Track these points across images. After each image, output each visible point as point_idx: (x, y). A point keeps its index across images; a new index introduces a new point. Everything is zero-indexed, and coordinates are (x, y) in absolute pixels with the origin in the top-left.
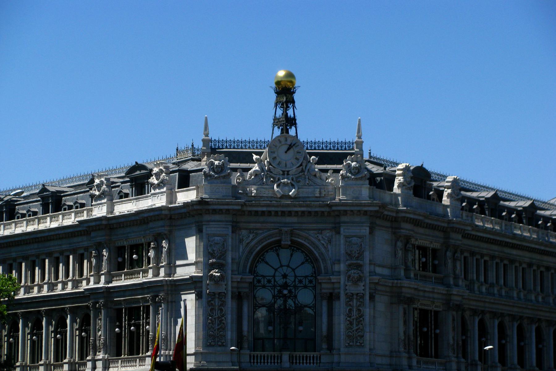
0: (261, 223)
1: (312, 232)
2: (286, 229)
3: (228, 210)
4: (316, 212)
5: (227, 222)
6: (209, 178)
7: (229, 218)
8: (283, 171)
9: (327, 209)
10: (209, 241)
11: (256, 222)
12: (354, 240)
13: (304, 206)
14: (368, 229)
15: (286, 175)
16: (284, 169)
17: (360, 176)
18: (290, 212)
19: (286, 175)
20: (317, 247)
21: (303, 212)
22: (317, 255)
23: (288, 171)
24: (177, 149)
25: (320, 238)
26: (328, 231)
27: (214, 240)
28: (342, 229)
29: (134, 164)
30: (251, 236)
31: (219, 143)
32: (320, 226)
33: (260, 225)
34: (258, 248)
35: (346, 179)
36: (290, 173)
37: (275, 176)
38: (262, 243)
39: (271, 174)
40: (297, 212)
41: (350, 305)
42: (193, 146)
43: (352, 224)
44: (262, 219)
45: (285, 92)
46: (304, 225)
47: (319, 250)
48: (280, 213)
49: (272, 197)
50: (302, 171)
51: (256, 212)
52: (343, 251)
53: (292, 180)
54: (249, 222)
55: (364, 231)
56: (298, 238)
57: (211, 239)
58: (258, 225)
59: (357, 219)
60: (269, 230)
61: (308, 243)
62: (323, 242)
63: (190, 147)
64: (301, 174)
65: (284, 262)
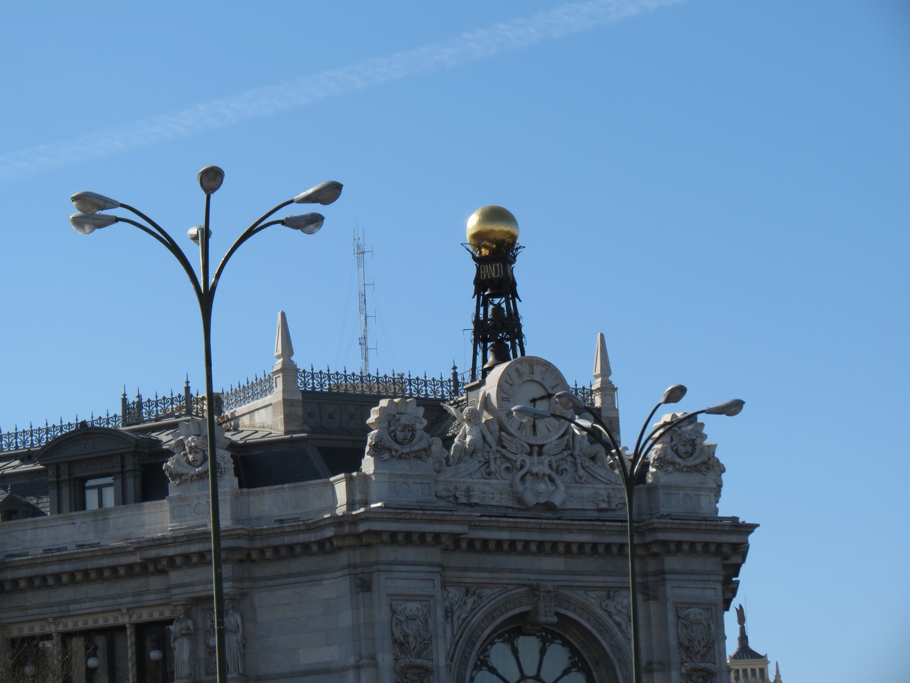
0: (492, 570)
1: (593, 594)
2: (550, 586)
3: (437, 536)
4: (608, 546)
5: (431, 565)
6: (386, 456)
7: (434, 555)
8: (531, 446)
10: (394, 612)
11: (479, 569)
12: (695, 613)
13: (588, 531)
14: (719, 587)
15: (535, 456)
16: (532, 442)
17: (698, 461)
18: (555, 544)
19: (535, 456)
21: (581, 545)
22: (608, 650)
23: (541, 447)
24: (124, 400)
25: (612, 609)
27: (405, 609)
28: (668, 587)
30: (470, 601)
31: (313, 378)
32: (611, 581)
33: (487, 575)
35: (671, 468)
36: (545, 449)
37: (513, 457)
38: (494, 619)
39: (504, 451)
40: (568, 545)
42: (187, 389)
43: (687, 577)
44: (492, 560)
45: (496, 262)
46: (579, 578)
48: (533, 548)
49: (507, 507)
50: (567, 447)
51: (485, 542)
52: (673, 642)
53: (550, 466)
54: (465, 569)
55: (712, 592)
56: (567, 609)
57: (400, 608)
59: (697, 563)
61: (589, 621)
62: (618, 619)
63: (183, 394)
64: (565, 453)
65: (530, 671)
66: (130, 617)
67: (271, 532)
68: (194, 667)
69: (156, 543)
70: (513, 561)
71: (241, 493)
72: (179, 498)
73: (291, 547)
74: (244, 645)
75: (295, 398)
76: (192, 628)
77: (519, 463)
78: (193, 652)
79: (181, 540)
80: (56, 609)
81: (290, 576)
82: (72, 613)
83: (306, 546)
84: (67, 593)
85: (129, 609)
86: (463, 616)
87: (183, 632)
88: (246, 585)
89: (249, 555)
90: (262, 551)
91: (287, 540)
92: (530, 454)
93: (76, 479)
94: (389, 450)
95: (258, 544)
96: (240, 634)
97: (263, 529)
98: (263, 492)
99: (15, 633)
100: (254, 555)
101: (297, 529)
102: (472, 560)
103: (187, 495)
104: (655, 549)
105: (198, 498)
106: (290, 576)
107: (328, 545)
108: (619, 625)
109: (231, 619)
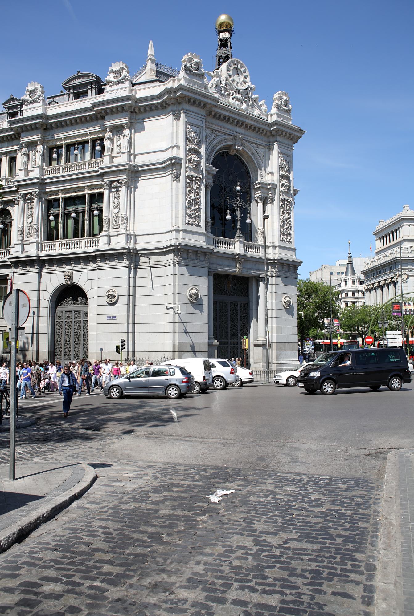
1: (252, 145)
9: (268, 128)
16: (237, 87)
20: (256, 158)
23: (239, 90)
26: (263, 147)
30: (213, 135)
32: (259, 142)
33: (219, 128)
34: (218, 148)
41: (283, 208)
44: (221, 123)
47: (258, 161)
54: (212, 124)
58: (218, 128)
59: (286, 141)
60: (225, 134)
62: (260, 155)
70: (228, 126)
77: (231, 94)
86: (211, 139)
92: (235, 92)
94: (190, 70)
100: (137, 111)
102: (215, 121)
104: (273, 133)
108: (260, 157)
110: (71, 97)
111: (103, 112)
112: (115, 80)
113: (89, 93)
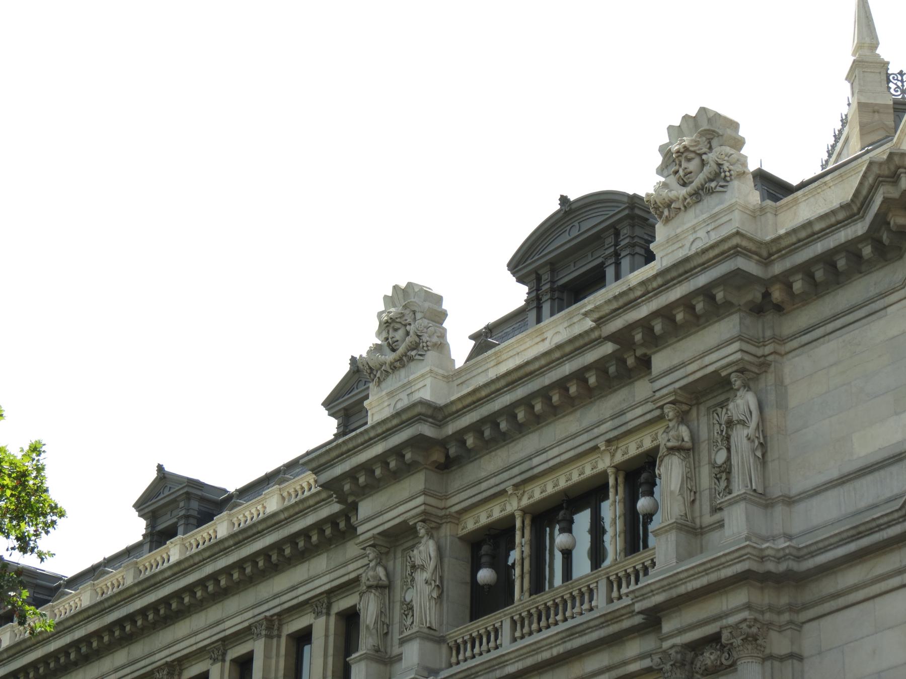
29: (556, 207)
66: (613, 456)
67: (794, 239)
68: (693, 501)
69: (621, 302)
71: (762, 209)
72: (669, 241)
73: (827, 259)
74: (763, 447)
75: (880, 101)
76: (687, 439)
78: (690, 478)
79: (655, 285)
80: (516, 471)
81: (835, 317)
82: (536, 471)
83: (850, 249)
84: (529, 444)
85: (609, 442)
87: (670, 444)
88: (768, 350)
89: (767, 295)
90: (785, 279)
91: (819, 248)
93: (564, 287)
95: (778, 268)
96: (753, 425)
97: (780, 238)
98: (796, 200)
99: (471, 524)
100: (777, 294)
101: (833, 220)
103: (679, 231)
105: (694, 229)
106: (835, 317)
107: (885, 238)
109: (739, 401)
110: (546, 307)
111: (638, 337)
112: (683, 191)
113: (610, 272)
